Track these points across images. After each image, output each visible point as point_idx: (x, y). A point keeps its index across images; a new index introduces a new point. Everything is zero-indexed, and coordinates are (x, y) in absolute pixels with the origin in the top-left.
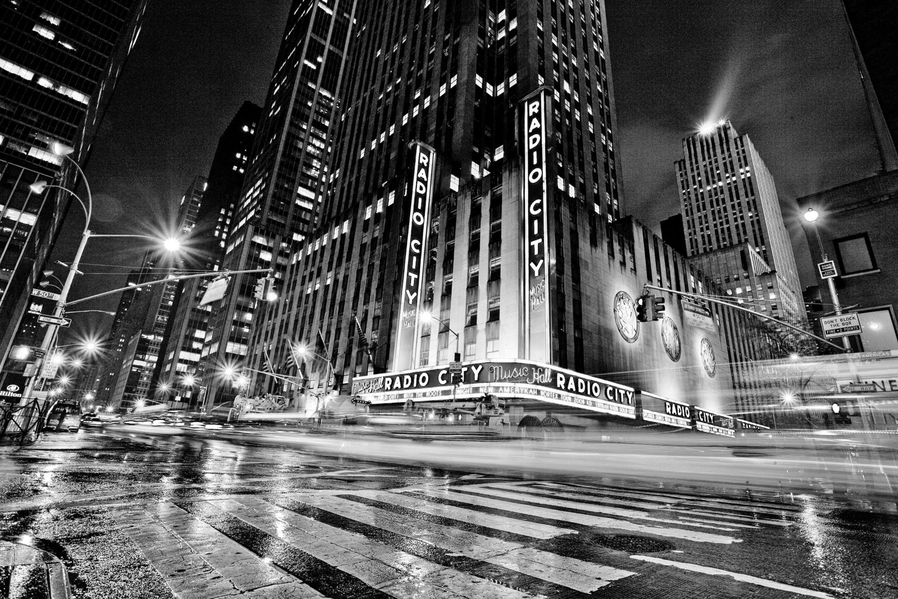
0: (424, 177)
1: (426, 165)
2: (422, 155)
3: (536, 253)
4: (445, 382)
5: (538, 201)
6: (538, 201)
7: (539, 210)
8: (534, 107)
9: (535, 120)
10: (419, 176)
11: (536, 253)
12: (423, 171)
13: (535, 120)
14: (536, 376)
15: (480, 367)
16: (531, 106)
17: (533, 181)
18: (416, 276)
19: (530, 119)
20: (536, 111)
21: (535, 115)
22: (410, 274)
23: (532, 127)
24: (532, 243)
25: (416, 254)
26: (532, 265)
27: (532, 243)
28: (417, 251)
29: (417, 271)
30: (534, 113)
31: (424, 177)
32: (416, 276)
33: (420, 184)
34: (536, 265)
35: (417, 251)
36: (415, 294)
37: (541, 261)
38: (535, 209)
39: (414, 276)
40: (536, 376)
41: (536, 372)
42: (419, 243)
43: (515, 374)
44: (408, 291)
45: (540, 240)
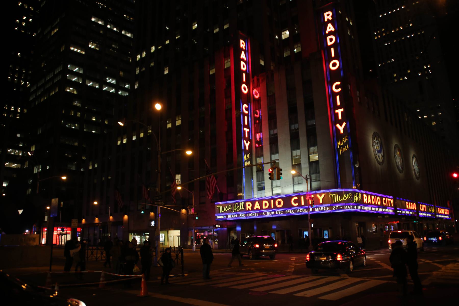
3: (340, 117)
4: (297, 204)
5: (339, 83)
6: (339, 83)
7: (340, 89)
8: (328, 15)
9: (330, 25)
11: (340, 117)
13: (330, 25)
16: (326, 14)
17: (333, 68)
19: (326, 24)
20: (330, 18)
22: (245, 129)
23: (328, 30)
24: (337, 111)
26: (338, 125)
27: (337, 111)
28: (246, 112)
29: (247, 127)
30: (328, 19)
34: (341, 126)
37: (344, 124)
38: (337, 87)
39: (247, 130)
45: (342, 110)
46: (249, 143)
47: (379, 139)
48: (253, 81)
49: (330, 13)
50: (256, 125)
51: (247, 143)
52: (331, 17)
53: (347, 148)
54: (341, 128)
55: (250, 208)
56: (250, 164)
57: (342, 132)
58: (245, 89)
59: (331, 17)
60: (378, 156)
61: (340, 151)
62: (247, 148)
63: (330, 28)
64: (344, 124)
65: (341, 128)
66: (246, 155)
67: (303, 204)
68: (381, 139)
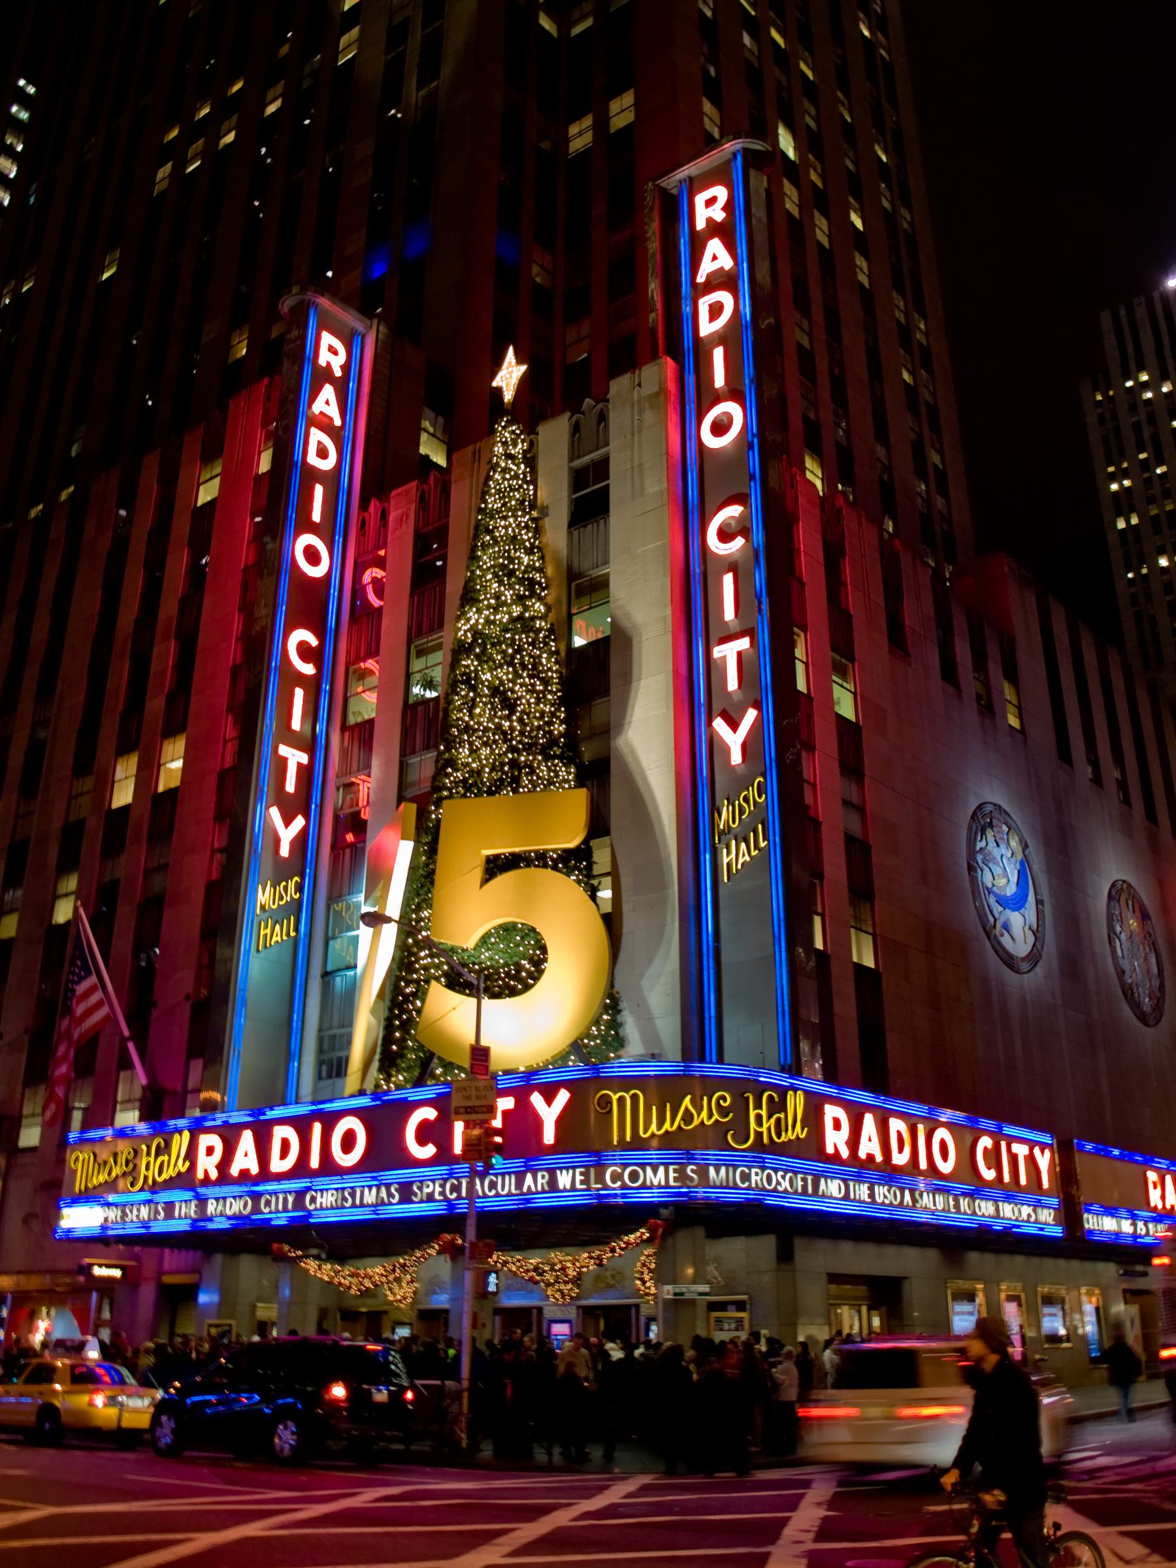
3: (732, 684)
4: (429, 1151)
8: (711, 202)
9: (715, 246)
13: (715, 246)
14: (759, 1119)
15: (563, 1096)
16: (700, 199)
18: (304, 758)
20: (719, 216)
21: (715, 229)
22: (284, 750)
23: (707, 267)
25: (300, 679)
26: (719, 725)
27: (718, 652)
30: (710, 220)
32: (304, 758)
34: (734, 726)
36: (299, 822)
37: (751, 715)
39: (295, 758)
40: (759, 1119)
41: (758, 1105)
42: (314, 642)
43: (688, 1117)
44: (274, 812)
45: (744, 643)
46: (299, 822)
47: (1014, 843)
48: (363, 525)
49: (721, 193)
50: (347, 734)
51: (287, 822)
52: (723, 209)
53: (756, 847)
54: (733, 740)
57: (736, 758)
58: (312, 556)
59: (723, 209)
60: (999, 925)
61: (726, 860)
62: (285, 851)
63: (715, 258)
64: (751, 715)
65: (733, 740)
67: (458, 1148)
68: (1025, 846)
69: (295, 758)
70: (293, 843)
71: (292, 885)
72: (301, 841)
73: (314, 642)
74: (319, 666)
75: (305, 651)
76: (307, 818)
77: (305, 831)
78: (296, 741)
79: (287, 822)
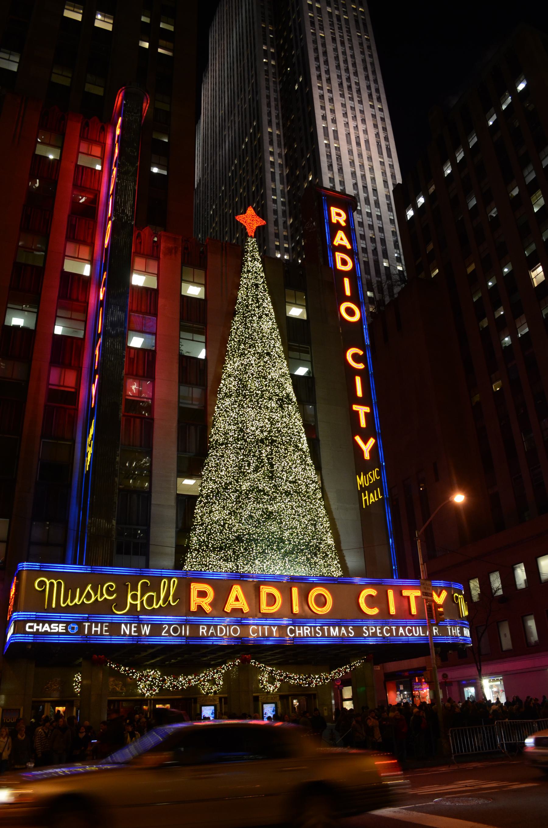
0: (346, 243)
1: (344, 224)
2: (334, 210)
10: (336, 243)
12: (340, 234)
18: (368, 410)
22: (355, 407)
28: (361, 366)
31: (346, 243)
32: (368, 410)
33: (339, 256)
35: (361, 366)
36: (372, 441)
39: (362, 410)
42: (361, 353)
44: (358, 439)
46: (372, 441)
51: (365, 442)
55: (206, 604)
56: (380, 497)
62: (367, 456)
66: (365, 474)
69: (362, 410)
70: (371, 452)
71: (375, 473)
72: (374, 451)
73: (361, 353)
74: (365, 364)
75: (355, 357)
76: (375, 438)
77: (375, 446)
78: (360, 402)
79: (365, 443)
